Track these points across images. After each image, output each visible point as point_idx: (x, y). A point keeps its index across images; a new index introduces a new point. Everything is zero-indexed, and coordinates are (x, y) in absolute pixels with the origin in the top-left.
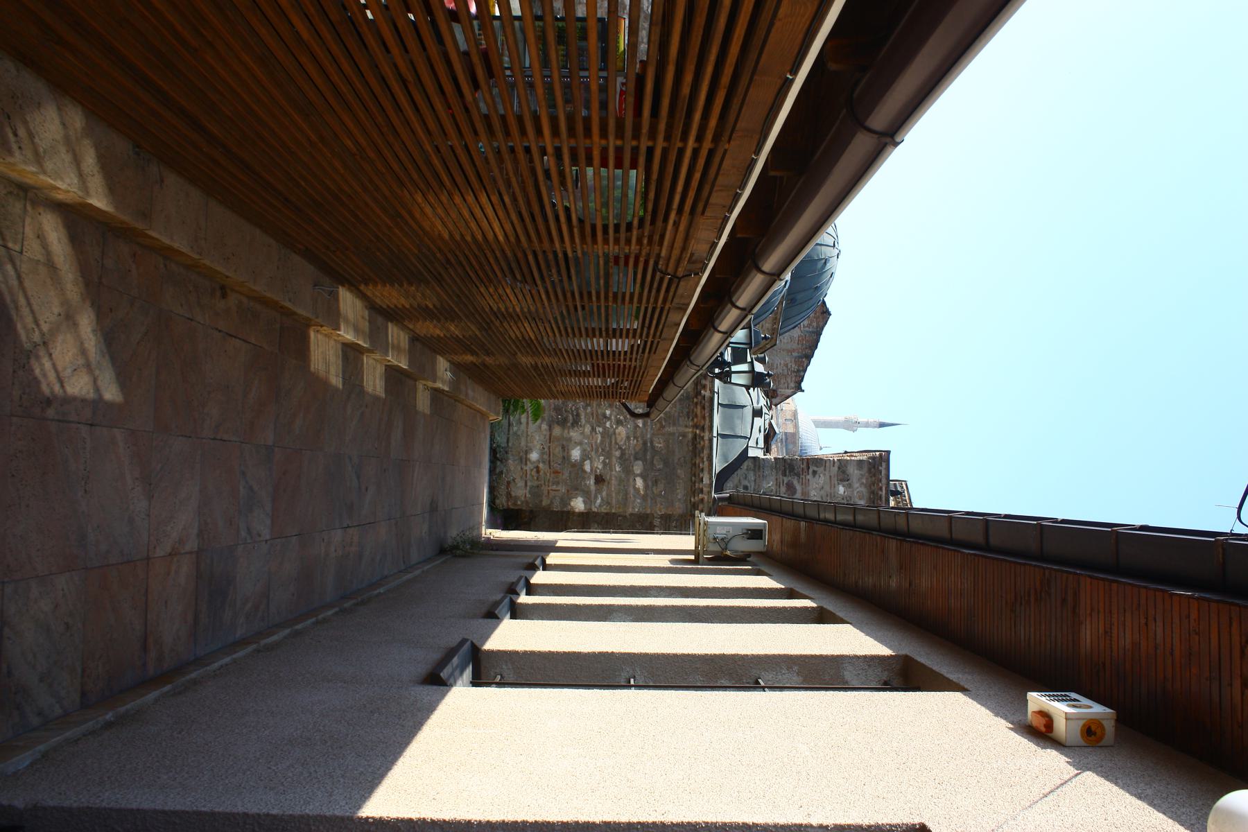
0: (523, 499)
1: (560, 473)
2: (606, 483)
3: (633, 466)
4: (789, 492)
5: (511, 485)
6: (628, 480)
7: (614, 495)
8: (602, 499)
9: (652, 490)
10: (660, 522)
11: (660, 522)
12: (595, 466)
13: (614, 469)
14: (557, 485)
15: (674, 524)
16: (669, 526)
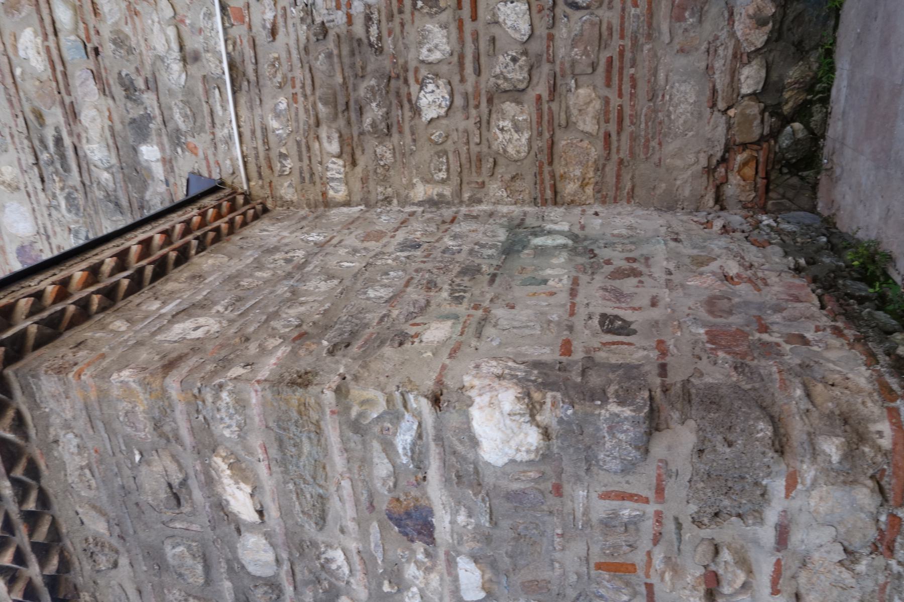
0: (808, 472)
1: (599, 566)
2: (383, 505)
3: (278, 561)
4: (33, 253)
5: (872, 534)
6: (285, 513)
7: (339, 461)
8: (388, 447)
9: (181, 467)
10: (327, 169)
11: (327, 169)
12: (434, 579)
13: (356, 559)
14: (615, 515)
15: (289, 163)
16: (301, 160)
